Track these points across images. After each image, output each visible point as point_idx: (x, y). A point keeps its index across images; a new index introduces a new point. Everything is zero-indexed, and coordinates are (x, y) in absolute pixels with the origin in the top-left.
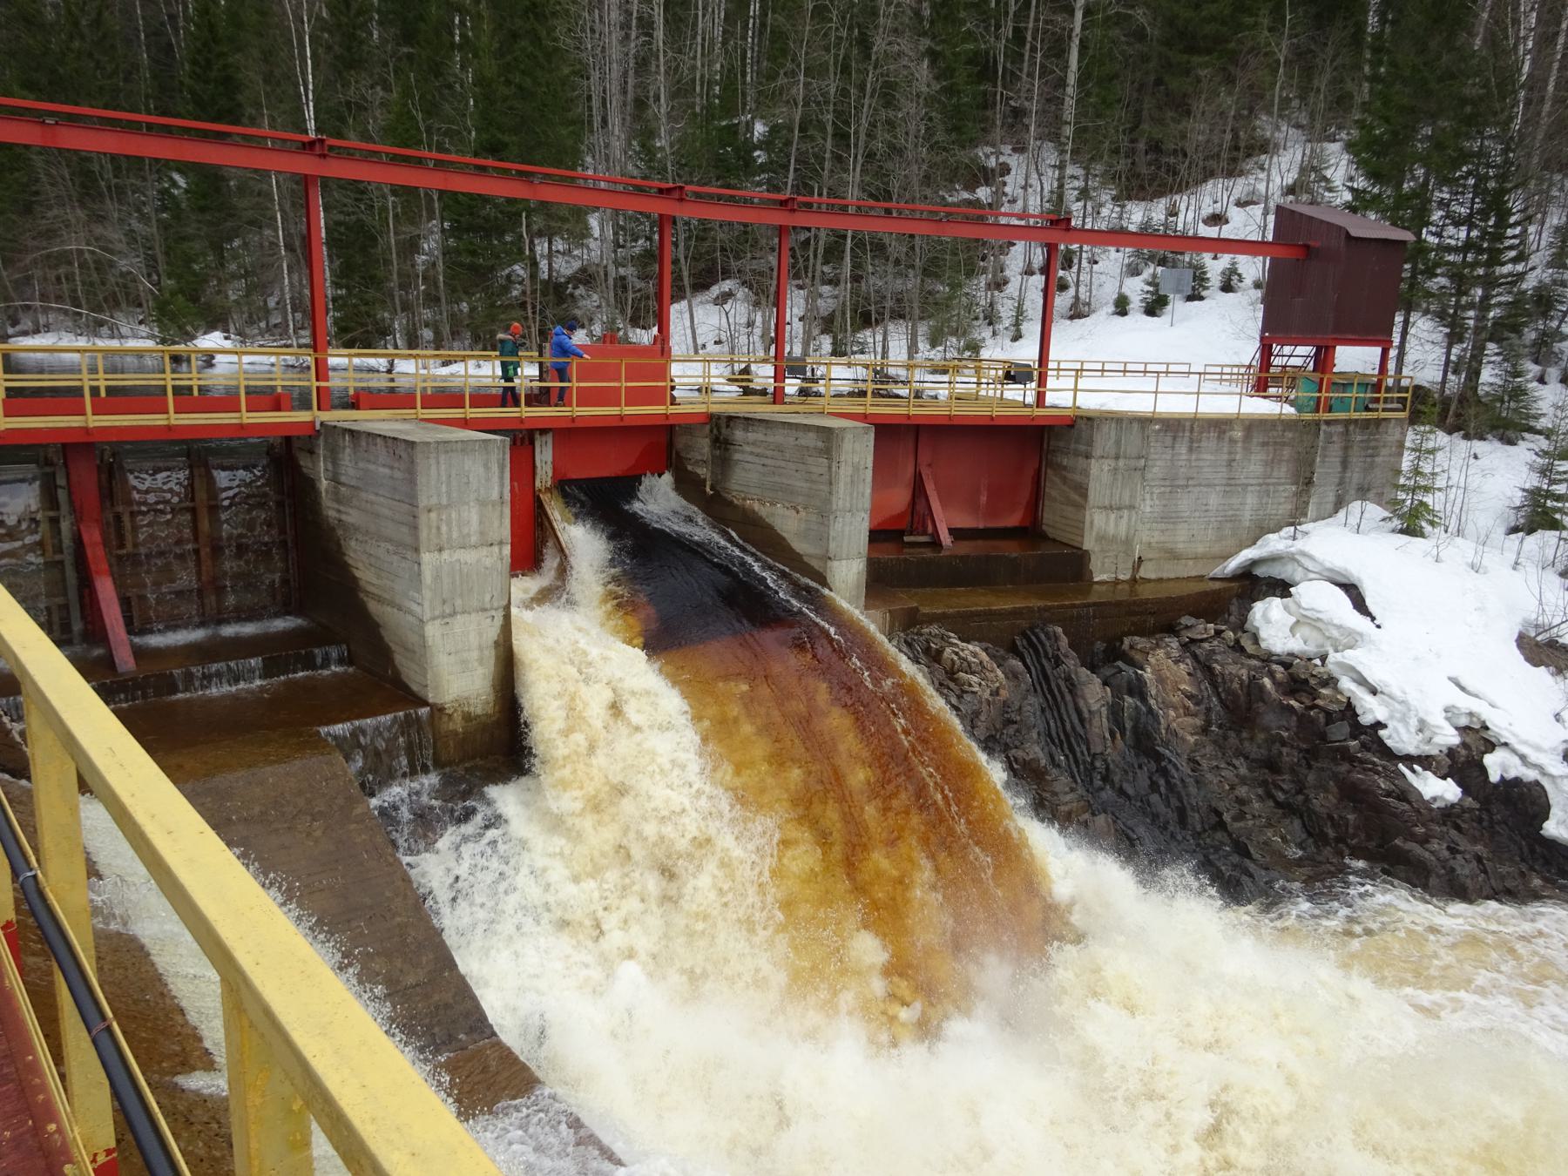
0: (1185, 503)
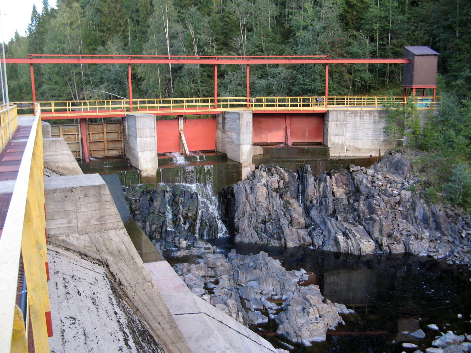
0: (360, 134)
